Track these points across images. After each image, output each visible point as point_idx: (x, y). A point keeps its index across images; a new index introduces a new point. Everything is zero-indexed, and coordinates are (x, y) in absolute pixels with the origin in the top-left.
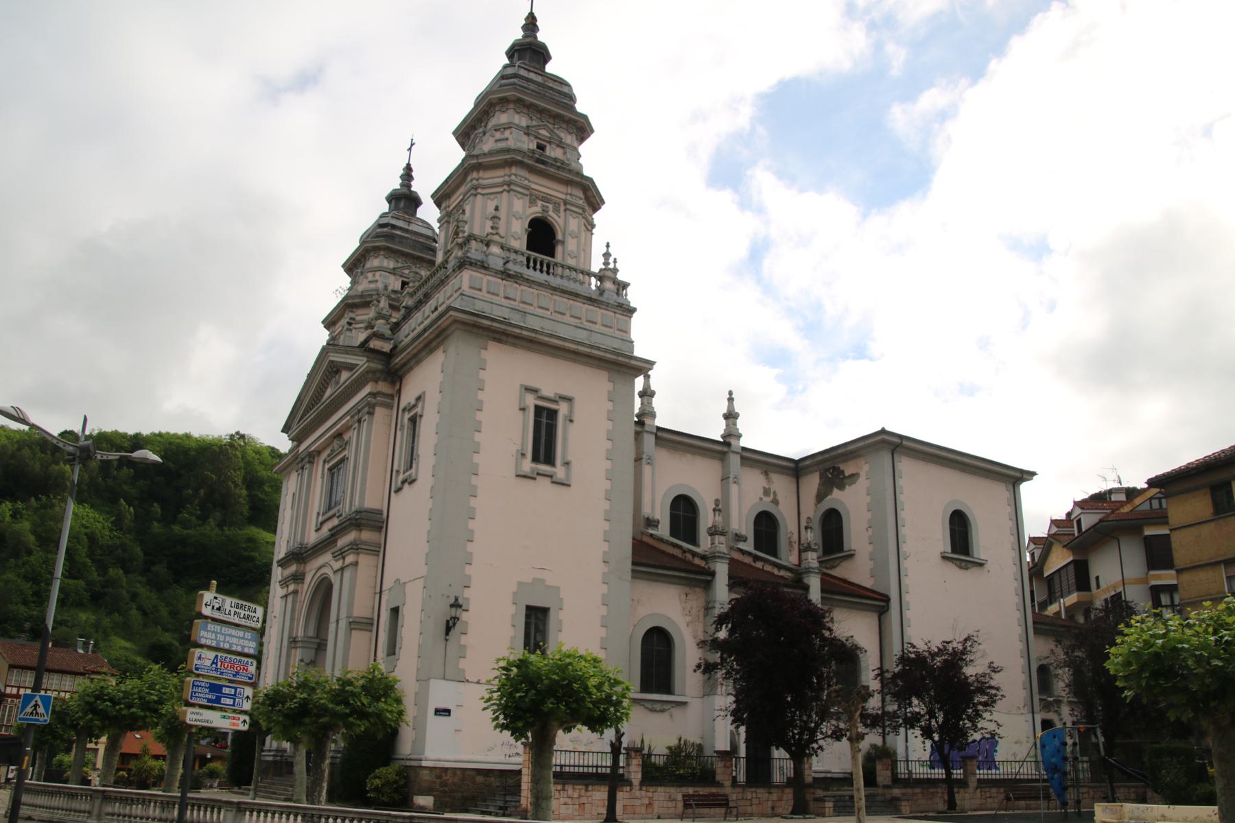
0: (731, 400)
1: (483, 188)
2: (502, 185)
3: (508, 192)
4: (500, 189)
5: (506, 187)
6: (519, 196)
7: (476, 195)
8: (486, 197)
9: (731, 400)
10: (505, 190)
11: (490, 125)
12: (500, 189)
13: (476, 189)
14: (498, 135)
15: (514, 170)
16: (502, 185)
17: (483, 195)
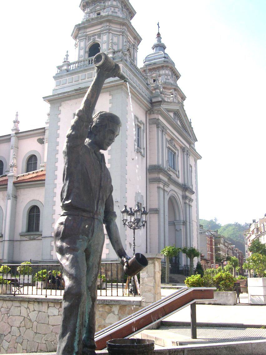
0: (17, 115)
1: (112, 31)
2: (120, 32)
3: (122, 36)
4: (119, 34)
5: (121, 33)
6: (116, 35)
7: (109, 33)
8: (113, 35)
9: (17, 115)
10: (121, 35)
11: (107, 4)
12: (119, 34)
13: (109, 30)
14: (112, 9)
15: (124, 27)
16: (120, 32)
17: (112, 33)
